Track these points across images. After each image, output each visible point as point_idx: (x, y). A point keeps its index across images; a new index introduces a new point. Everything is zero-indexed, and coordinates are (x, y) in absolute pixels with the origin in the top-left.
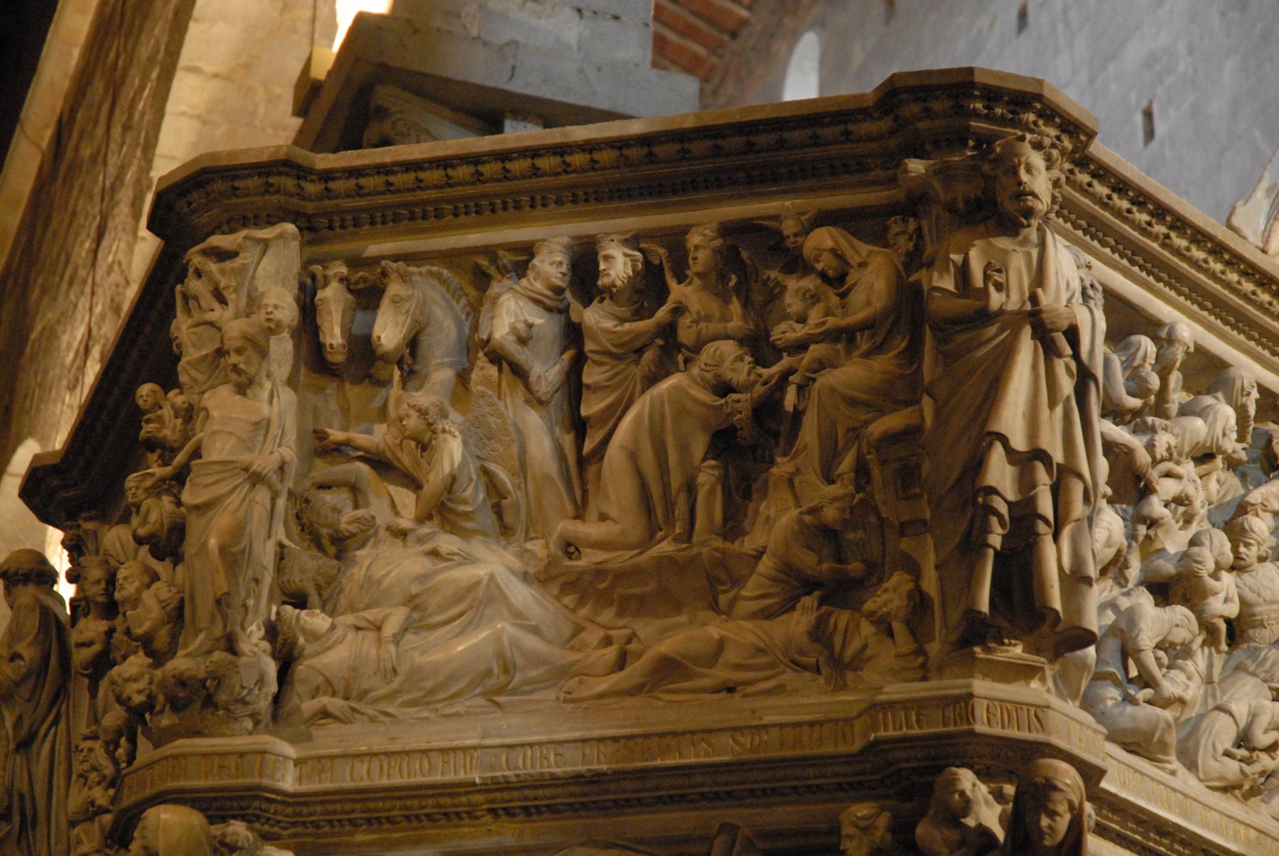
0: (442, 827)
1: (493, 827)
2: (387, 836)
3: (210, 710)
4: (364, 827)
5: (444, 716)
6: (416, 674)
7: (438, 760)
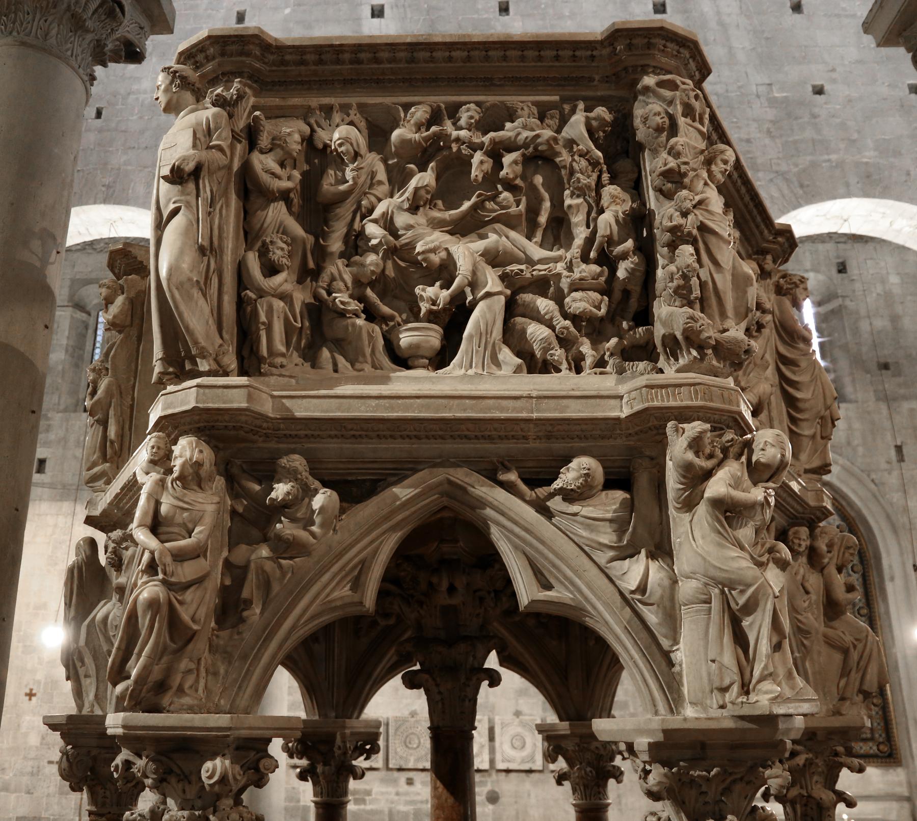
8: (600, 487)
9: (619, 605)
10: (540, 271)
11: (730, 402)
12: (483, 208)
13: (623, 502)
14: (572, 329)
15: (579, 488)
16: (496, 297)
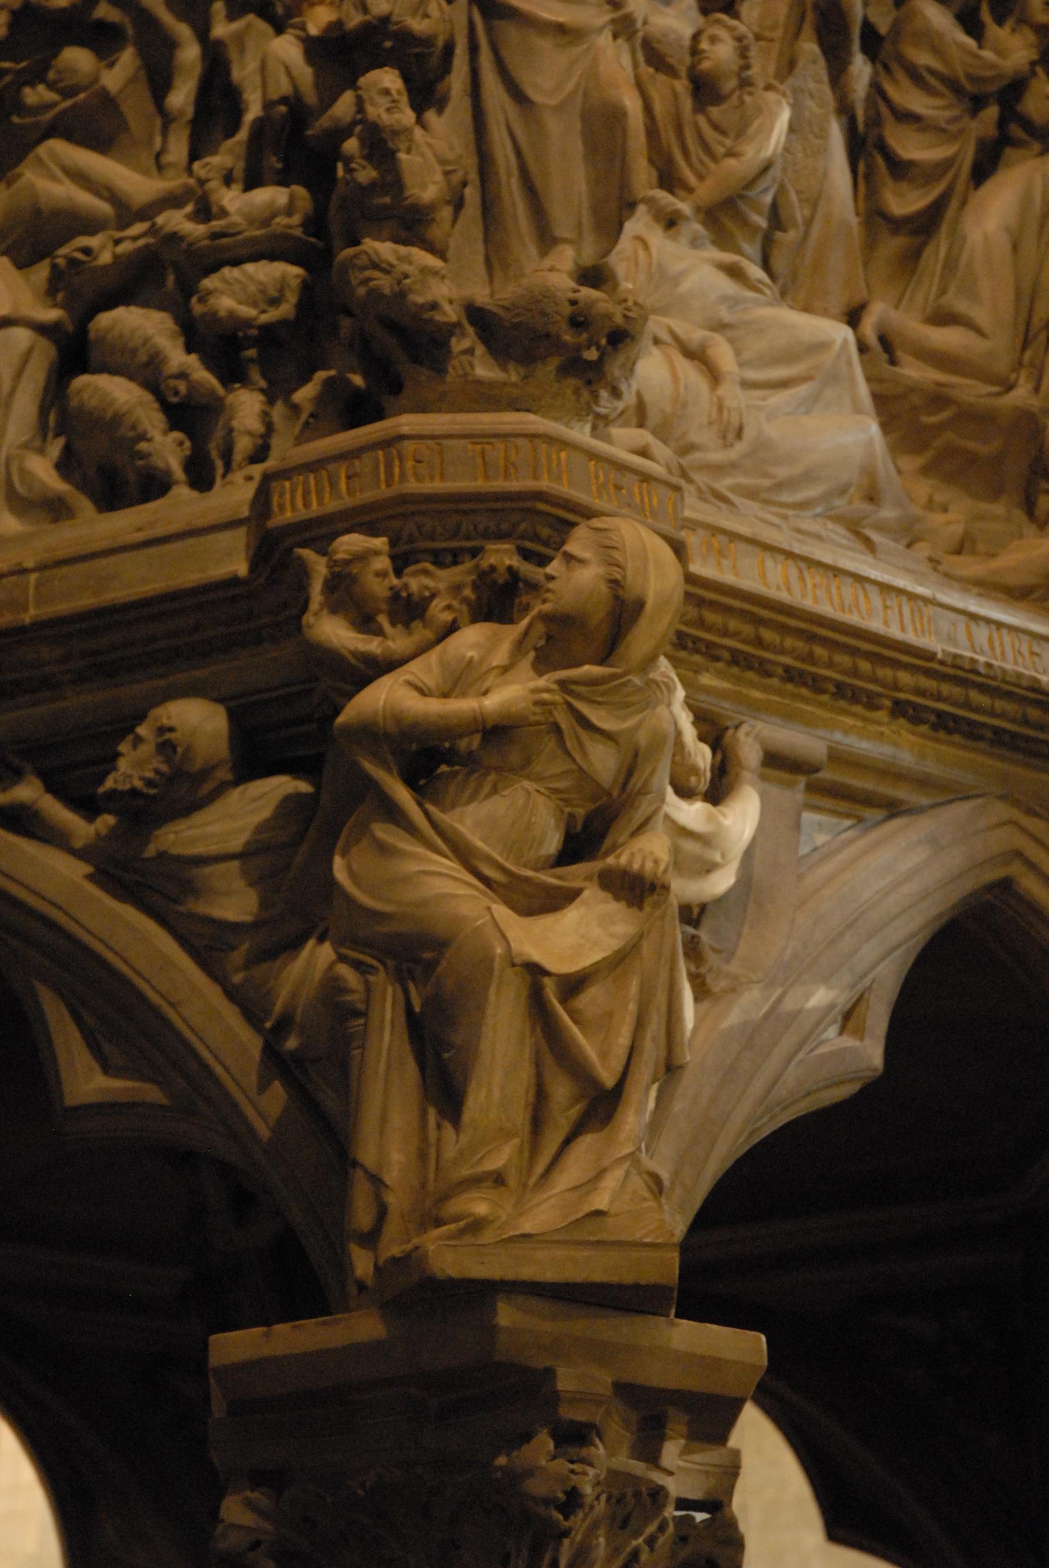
0: (821, 705)
2: (744, 691)
3: (579, 383)
4: (720, 665)
5: (799, 531)
6: (762, 445)
7: (876, 599)
8: (223, 774)
9: (254, 1079)
10: (135, 239)
13: (290, 805)
14: (203, 376)
15: (149, 783)
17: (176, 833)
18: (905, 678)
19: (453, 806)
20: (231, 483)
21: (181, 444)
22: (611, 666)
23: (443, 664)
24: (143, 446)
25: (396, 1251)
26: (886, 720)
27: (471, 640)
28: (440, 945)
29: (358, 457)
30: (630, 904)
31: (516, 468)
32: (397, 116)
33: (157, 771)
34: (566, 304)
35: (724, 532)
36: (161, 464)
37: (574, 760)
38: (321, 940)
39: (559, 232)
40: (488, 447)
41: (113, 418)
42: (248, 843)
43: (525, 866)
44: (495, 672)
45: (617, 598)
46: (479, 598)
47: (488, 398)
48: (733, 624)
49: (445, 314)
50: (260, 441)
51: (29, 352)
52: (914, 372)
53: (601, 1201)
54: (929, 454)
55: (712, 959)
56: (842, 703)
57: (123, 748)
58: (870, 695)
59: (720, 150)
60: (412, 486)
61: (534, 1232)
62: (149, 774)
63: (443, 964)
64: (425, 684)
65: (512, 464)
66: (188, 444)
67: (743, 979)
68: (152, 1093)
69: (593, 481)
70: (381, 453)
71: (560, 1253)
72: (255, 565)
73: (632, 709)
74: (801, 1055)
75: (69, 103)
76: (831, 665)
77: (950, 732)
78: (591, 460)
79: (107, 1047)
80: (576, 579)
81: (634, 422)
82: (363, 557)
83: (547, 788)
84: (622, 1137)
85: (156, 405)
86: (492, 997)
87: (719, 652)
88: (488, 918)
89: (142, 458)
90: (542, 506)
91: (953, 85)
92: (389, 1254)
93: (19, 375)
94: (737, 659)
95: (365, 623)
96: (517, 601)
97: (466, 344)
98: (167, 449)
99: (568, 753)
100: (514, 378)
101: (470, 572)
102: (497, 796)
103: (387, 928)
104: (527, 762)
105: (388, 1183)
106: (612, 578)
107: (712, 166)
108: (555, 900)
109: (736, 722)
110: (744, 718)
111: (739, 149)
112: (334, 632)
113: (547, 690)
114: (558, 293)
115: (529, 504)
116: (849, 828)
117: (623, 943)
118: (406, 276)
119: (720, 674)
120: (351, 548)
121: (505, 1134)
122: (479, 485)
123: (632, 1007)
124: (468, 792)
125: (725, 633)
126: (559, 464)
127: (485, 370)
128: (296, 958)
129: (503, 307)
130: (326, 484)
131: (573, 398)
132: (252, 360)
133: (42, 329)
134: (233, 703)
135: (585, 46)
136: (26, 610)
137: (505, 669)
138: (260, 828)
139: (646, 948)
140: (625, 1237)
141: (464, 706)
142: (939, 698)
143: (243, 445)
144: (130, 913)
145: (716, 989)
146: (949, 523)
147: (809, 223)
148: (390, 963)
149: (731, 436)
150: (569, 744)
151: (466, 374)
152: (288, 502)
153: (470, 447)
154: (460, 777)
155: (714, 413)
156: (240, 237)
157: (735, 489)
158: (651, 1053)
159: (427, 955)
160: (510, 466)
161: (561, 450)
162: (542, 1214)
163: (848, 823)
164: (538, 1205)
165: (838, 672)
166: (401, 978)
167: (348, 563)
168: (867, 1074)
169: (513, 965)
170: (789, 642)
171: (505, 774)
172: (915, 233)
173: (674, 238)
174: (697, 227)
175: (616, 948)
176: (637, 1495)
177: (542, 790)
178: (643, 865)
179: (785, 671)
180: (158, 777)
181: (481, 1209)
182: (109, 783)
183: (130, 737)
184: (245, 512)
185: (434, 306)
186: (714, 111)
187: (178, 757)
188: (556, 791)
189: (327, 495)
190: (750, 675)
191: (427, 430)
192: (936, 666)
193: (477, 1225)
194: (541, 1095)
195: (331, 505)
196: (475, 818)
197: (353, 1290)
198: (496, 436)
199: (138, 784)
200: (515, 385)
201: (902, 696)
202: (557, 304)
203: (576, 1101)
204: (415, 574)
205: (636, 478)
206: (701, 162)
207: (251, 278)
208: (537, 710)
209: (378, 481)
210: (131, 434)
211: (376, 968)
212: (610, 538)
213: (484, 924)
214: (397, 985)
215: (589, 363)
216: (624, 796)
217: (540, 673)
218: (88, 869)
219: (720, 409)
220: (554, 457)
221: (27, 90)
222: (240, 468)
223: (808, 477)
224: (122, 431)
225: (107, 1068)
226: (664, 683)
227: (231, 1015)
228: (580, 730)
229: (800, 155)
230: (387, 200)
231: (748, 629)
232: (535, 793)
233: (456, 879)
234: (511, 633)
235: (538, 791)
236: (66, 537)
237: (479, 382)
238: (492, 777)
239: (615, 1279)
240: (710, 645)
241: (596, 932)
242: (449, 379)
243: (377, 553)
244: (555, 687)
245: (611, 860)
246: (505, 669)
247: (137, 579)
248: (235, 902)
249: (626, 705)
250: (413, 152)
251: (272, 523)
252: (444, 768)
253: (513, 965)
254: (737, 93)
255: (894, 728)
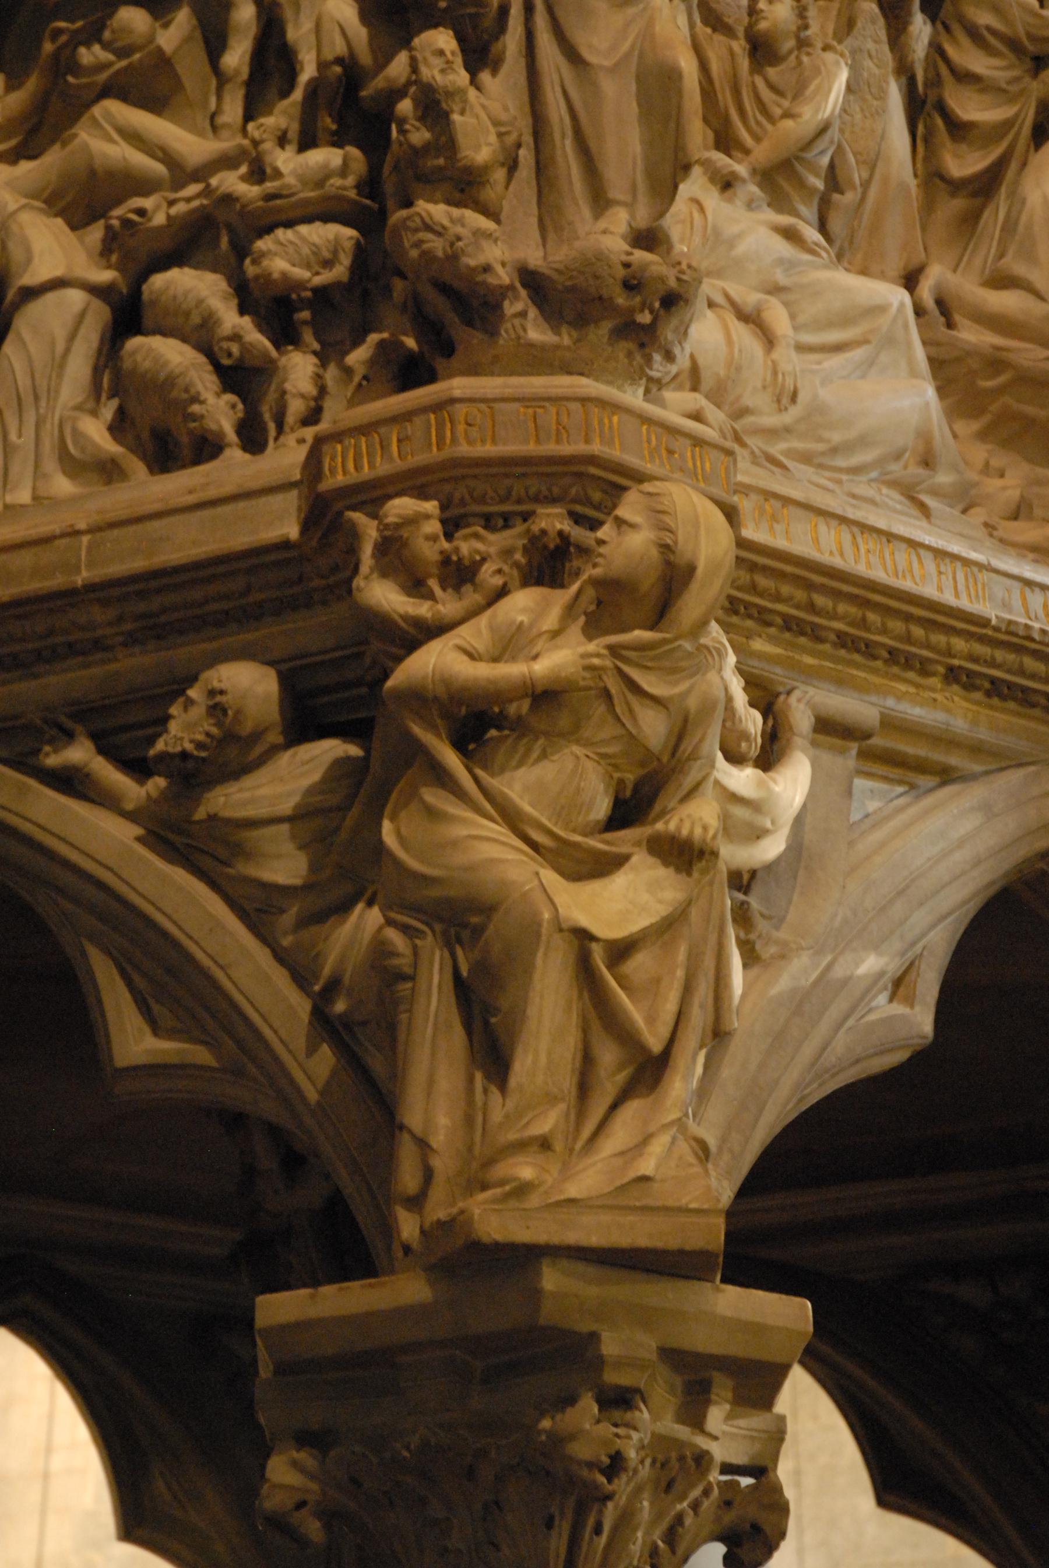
0: (875, 671)
1: (938, 696)
2: (797, 657)
3: (630, 345)
4: (773, 630)
5: (854, 496)
6: (818, 409)
7: (930, 564)
8: (275, 737)
10: (188, 200)
11: (561, 433)
12: (75, 68)
13: (340, 767)
14: (257, 338)
15: (200, 746)
16: (51, 297)
17: (226, 795)
18: (959, 644)
19: (502, 770)
20: (284, 445)
21: (233, 406)
22: (661, 632)
23: (492, 628)
24: (196, 408)
25: (442, 1214)
26: (939, 686)
27: (521, 604)
28: (489, 910)
29: (410, 421)
30: (678, 870)
31: (567, 431)
32: (451, 77)
33: (208, 734)
34: (620, 267)
35: (776, 496)
36: (213, 427)
37: (623, 725)
38: (370, 904)
39: (614, 194)
40: (540, 411)
41: (166, 379)
42: (297, 807)
43: (574, 831)
44: (545, 637)
45: (668, 564)
46: (530, 563)
47: (539, 361)
48: (786, 590)
49: (499, 277)
50: (313, 404)
51: (82, 315)
52: (971, 335)
53: (647, 1166)
54: (986, 419)
55: (762, 926)
56: (895, 670)
57: (174, 710)
58: (924, 662)
59: (777, 111)
60: (464, 449)
61: (578, 1196)
62: (200, 737)
63: (491, 929)
64: (474, 648)
65: (564, 428)
66: (240, 406)
67: (793, 946)
68: (202, 1055)
69: (646, 445)
70: (432, 416)
71: (605, 1218)
72: (306, 527)
73: (683, 674)
74: (851, 1022)
75: (124, 63)
76: (884, 631)
77: (1003, 698)
78: (643, 423)
79: (156, 1008)
80: (627, 544)
81: (688, 385)
82: (414, 520)
83: (598, 754)
84: (669, 1102)
85: (210, 368)
86: (539, 961)
87: (769, 617)
88: (536, 882)
89: (195, 421)
90: (593, 470)
91: (1014, 45)
92: (435, 1218)
93: (72, 338)
94: (789, 624)
95: (416, 587)
96: (567, 565)
97: (519, 306)
98: (220, 411)
99: (619, 719)
100: (566, 341)
101: (520, 536)
102: (545, 763)
103: (435, 892)
104: (577, 727)
105: (435, 1146)
106: (663, 542)
107: (769, 127)
108: (604, 866)
109: (788, 687)
110: (795, 684)
111: (796, 110)
112: (385, 596)
113: (598, 655)
114: (612, 256)
115: (582, 468)
116: (902, 795)
117: (671, 909)
118: (459, 239)
119: (772, 640)
120: (401, 512)
121: (552, 1099)
122: (531, 448)
123: (680, 973)
124: (517, 757)
125: (778, 598)
126: (611, 427)
127: (537, 333)
128: (345, 921)
129: (556, 270)
130: (378, 447)
131: (626, 360)
132: (305, 323)
133: (95, 290)
134: (284, 667)
135: (641, 6)
136: (77, 570)
137: (555, 634)
138: (310, 791)
139: (694, 913)
140: (670, 1203)
141: (513, 670)
142: (992, 664)
143: (296, 408)
144: (180, 875)
145: (765, 955)
146: (1004, 488)
147: (866, 185)
148: (438, 927)
149: (785, 401)
150: (618, 710)
151: (519, 338)
152: (340, 465)
153: (522, 410)
154: (510, 741)
155: (769, 378)
156: (293, 199)
157: (789, 453)
158: (699, 1018)
159: (475, 920)
160: (563, 431)
161: (614, 414)
162: (588, 1179)
163: (900, 789)
164: (585, 1169)
165: (891, 638)
166: (449, 944)
167: (398, 526)
168: (920, 1041)
169: (561, 930)
170: (842, 608)
171: (555, 739)
172: (975, 194)
173: (730, 200)
174: (754, 189)
175: (664, 913)
176: (682, 1458)
177: (591, 755)
178: (691, 832)
179: (838, 637)
180: (209, 740)
181: (527, 1173)
182: (160, 746)
183: (181, 700)
184: (298, 477)
185: (487, 269)
186: (771, 72)
187: (228, 721)
188: (604, 756)
189: (379, 459)
190: (802, 640)
191: (480, 393)
192: (990, 632)
193: (522, 1190)
194: (587, 1060)
195: (383, 468)
196: (526, 783)
197: (400, 1254)
198: (549, 399)
199: (189, 746)
200: (568, 348)
201: (956, 662)
202: (610, 267)
203: (621, 1067)
204: (466, 538)
205: (688, 442)
206: (758, 123)
207: (303, 239)
208: (587, 675)
209: (430, 444)
210: (185, 396)
211: (423, 932)
212: (662, 503)
213: (531, 890)
214: (445, 950)
215: (642, 327)
216: (674, 762)
217: (590, 638)
218: (139, 831)
219: (775, 373)
220: (606, 421)
221: (82, 50)
222: (292, 430)
223: (863, 441)
224: (175, 394)
225: (156, 1030)
226: (715, 648)
227: (280, 977)
228: (630, 696)
229: (858, 116)
230: (441, 161)
231: (800, 595)
232: (583, 758)
233: (503, 843)
234: (561, 597)
235: (587, 756)
236: (118, 499)
237: (531, 345)
238: (541, 741)
239: (659, 1244)
240: (762, 610)
241: (645, 897)
242: (501, 342)
243: (427, 517)
244: (605, 652)
245: (659, 826)
246: (555, 634)
247: (188, 542)
248: (284, 865)
249: (673, 671)
250: (468, 112)
251: (324, 486)
252: (493, 733)
253: (561, 930)
254: (796, 53)
255: (947, 694)
